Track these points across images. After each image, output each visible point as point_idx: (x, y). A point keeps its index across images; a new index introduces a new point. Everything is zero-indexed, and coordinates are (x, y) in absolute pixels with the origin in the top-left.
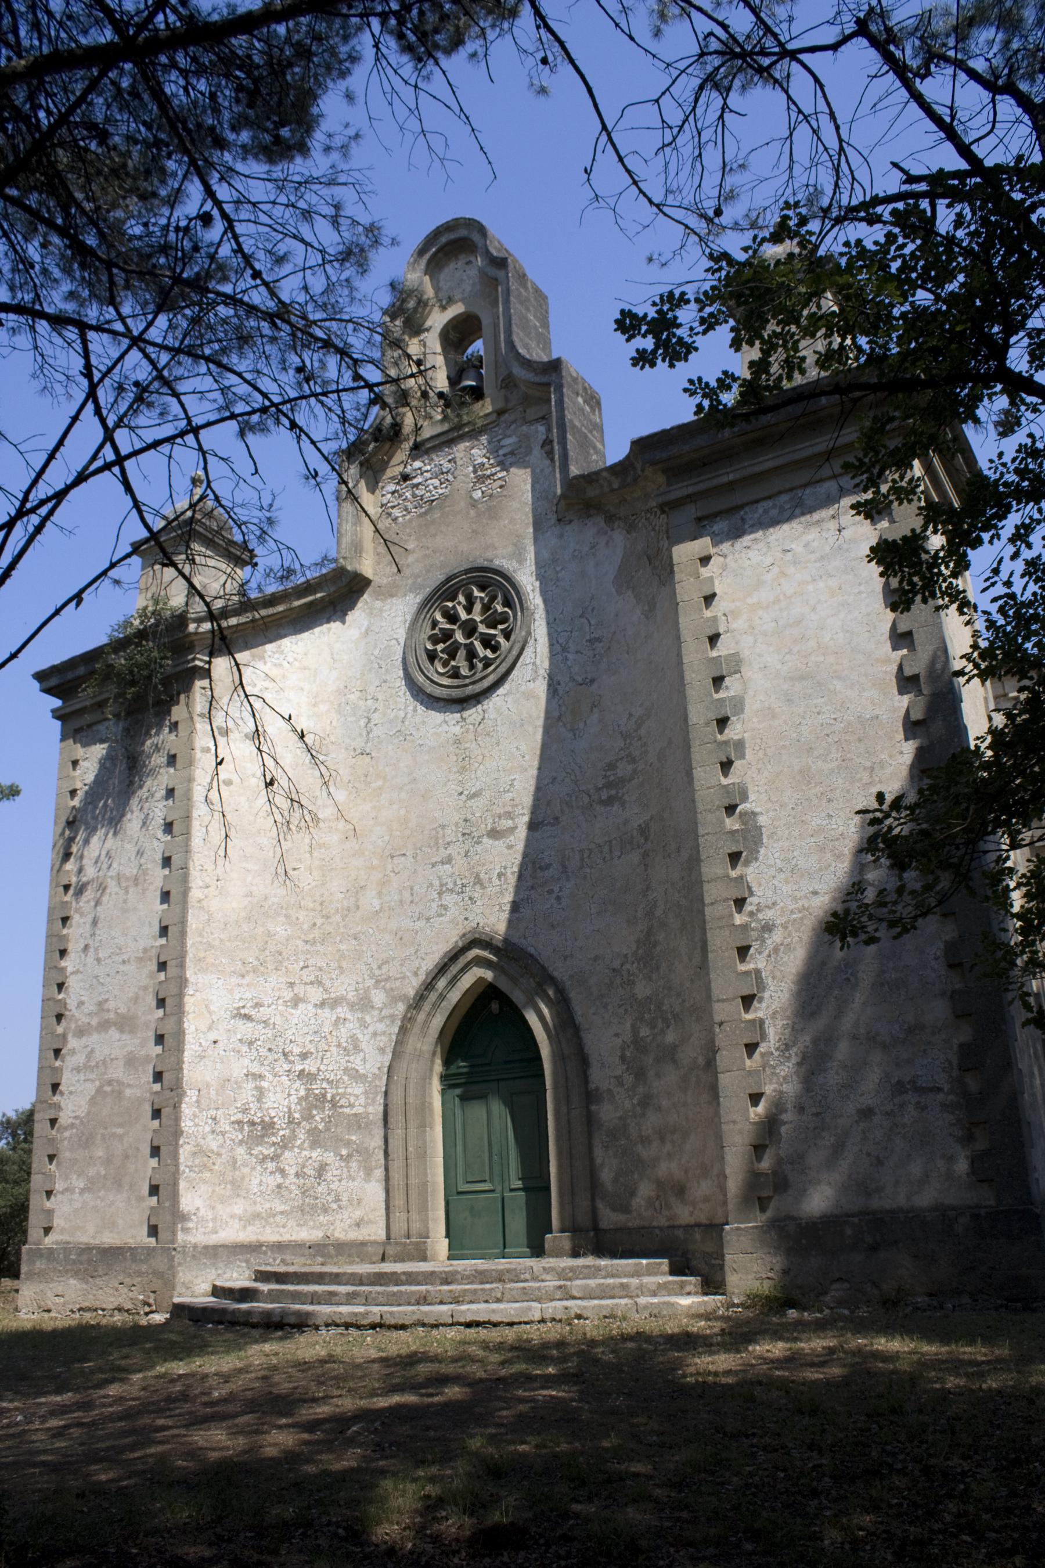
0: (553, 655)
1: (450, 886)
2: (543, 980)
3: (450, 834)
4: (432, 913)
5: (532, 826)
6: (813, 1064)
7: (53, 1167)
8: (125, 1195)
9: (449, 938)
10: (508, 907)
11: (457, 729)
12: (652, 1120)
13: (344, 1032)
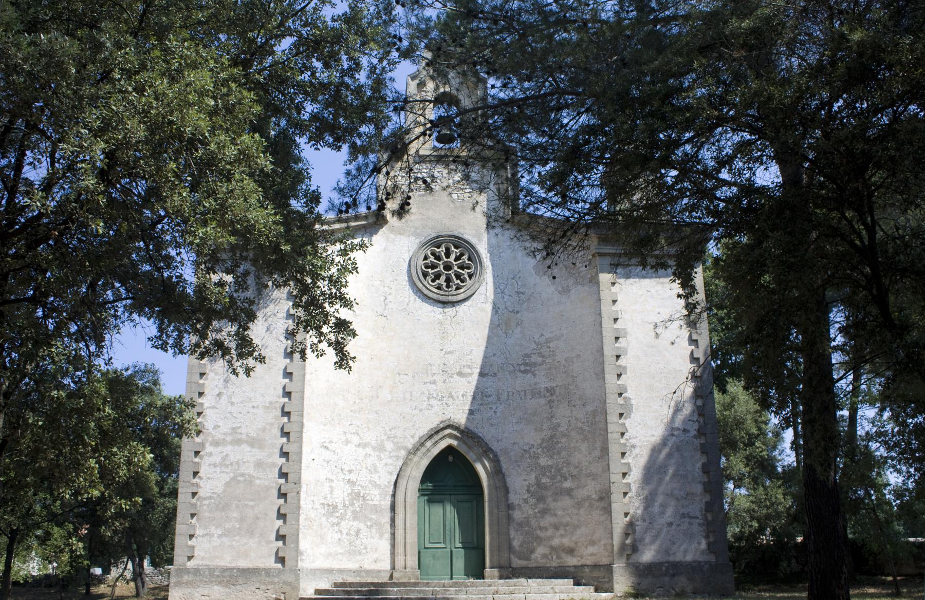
0: (495, 293)
1: (435, 395)
2: (487, 451)
3: (435, 369)
4: (424, 407)
5: (482, 374)
6: (648, 502)
7: (194, 521)
8: (256, 540)
9: (433, 422)
10: (467, 412)
11: (440, 317)
12: (548, 520)
13: (369, 461)
